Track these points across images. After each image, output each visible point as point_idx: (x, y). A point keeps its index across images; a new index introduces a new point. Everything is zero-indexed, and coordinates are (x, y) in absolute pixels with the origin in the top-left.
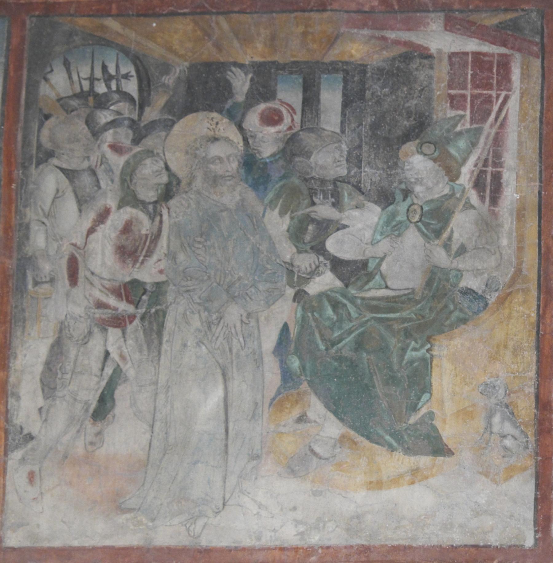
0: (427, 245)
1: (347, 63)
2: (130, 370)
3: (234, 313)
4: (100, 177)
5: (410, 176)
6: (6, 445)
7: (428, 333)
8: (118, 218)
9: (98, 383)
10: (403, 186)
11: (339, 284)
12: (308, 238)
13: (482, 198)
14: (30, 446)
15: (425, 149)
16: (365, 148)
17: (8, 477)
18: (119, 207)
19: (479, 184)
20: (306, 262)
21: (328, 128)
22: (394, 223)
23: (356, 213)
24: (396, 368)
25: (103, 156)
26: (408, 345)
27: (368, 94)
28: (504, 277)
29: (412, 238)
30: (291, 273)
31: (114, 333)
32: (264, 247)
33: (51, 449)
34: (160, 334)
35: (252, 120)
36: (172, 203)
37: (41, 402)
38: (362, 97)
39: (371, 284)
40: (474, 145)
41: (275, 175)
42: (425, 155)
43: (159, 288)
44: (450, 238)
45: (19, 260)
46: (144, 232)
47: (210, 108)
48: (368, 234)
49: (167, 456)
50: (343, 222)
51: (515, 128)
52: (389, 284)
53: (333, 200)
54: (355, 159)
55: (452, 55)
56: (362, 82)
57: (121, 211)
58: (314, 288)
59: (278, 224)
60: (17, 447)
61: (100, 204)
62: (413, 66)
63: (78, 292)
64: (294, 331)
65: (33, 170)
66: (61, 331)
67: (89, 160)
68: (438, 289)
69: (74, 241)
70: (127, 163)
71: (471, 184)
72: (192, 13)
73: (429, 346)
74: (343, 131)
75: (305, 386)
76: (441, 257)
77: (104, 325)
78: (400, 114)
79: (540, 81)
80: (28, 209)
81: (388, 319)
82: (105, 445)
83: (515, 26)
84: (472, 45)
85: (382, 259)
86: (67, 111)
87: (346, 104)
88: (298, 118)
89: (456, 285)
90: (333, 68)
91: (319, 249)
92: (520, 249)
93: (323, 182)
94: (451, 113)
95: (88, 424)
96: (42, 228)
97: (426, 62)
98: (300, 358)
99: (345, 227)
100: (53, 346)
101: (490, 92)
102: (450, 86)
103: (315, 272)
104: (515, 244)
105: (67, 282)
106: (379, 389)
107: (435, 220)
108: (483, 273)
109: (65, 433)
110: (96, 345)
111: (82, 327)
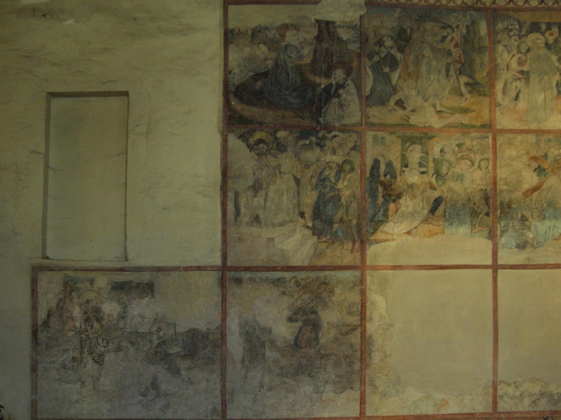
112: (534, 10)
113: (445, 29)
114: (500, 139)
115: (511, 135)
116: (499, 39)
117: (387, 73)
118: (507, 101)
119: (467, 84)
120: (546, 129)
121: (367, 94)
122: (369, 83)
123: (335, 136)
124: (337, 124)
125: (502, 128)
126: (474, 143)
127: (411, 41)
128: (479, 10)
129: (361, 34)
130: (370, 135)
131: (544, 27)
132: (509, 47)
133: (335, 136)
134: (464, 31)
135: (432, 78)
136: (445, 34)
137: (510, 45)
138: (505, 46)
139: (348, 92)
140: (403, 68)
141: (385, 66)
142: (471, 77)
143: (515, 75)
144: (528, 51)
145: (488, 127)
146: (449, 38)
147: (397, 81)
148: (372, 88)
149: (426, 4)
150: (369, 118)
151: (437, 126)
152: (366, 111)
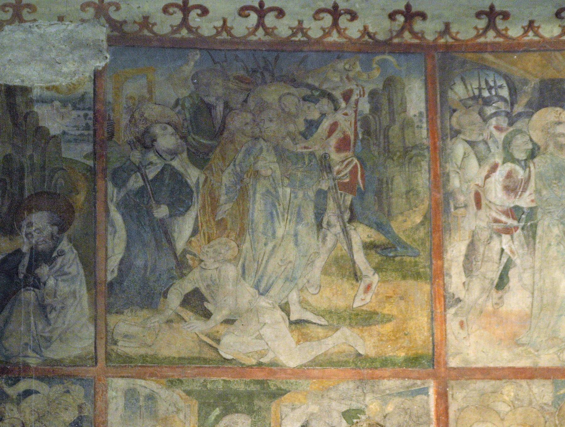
2: (517, 261)
6: (445, 305)
9: (498, 267)
14: (459, 305)
17: (447, 324)
18: (504, 163)
31: (506, 238)
33: (472, 307)
34: (534, 238)
37: (464, 279)
43: (532, 212)
45: (445, 194)
46: (520, 177)
49: (543, 312)
57: (505, 165)
60: (451, 306)
63: (482, 213)
66: (473, 236)
67: (482, 135)
69: (477, 183)
77: (499, 233)
80: (447, 165)
82: (505, 305)
86: (466, 107)
95: (494, 292)
96: (457, 175)
100: (469, 246)
105: (475, 208)
109: (479, 298)
110: (496, 245)
111: (486, 234)
113: (315, 101)
117: (162, 220)
118: (476, 291)
121: (109, 278)
122: (115, 247)
123: (27, 393)
124: (33, 361)
126: (390, 408)
127: (225, 134)
129: (96, 120)
130: (117, 386)
133: (27, 393)
135: (280, 232)
136: (315, 115)
137: (486, 143)
139: (61, 273)
140: (204, 207)
141: (158, 203)
146: (326, 124)
147: (189, 242)
148: (121, 262)
149: (267, 38)
150: (116, 343)
151: (293, 363)
152: (106, 325)
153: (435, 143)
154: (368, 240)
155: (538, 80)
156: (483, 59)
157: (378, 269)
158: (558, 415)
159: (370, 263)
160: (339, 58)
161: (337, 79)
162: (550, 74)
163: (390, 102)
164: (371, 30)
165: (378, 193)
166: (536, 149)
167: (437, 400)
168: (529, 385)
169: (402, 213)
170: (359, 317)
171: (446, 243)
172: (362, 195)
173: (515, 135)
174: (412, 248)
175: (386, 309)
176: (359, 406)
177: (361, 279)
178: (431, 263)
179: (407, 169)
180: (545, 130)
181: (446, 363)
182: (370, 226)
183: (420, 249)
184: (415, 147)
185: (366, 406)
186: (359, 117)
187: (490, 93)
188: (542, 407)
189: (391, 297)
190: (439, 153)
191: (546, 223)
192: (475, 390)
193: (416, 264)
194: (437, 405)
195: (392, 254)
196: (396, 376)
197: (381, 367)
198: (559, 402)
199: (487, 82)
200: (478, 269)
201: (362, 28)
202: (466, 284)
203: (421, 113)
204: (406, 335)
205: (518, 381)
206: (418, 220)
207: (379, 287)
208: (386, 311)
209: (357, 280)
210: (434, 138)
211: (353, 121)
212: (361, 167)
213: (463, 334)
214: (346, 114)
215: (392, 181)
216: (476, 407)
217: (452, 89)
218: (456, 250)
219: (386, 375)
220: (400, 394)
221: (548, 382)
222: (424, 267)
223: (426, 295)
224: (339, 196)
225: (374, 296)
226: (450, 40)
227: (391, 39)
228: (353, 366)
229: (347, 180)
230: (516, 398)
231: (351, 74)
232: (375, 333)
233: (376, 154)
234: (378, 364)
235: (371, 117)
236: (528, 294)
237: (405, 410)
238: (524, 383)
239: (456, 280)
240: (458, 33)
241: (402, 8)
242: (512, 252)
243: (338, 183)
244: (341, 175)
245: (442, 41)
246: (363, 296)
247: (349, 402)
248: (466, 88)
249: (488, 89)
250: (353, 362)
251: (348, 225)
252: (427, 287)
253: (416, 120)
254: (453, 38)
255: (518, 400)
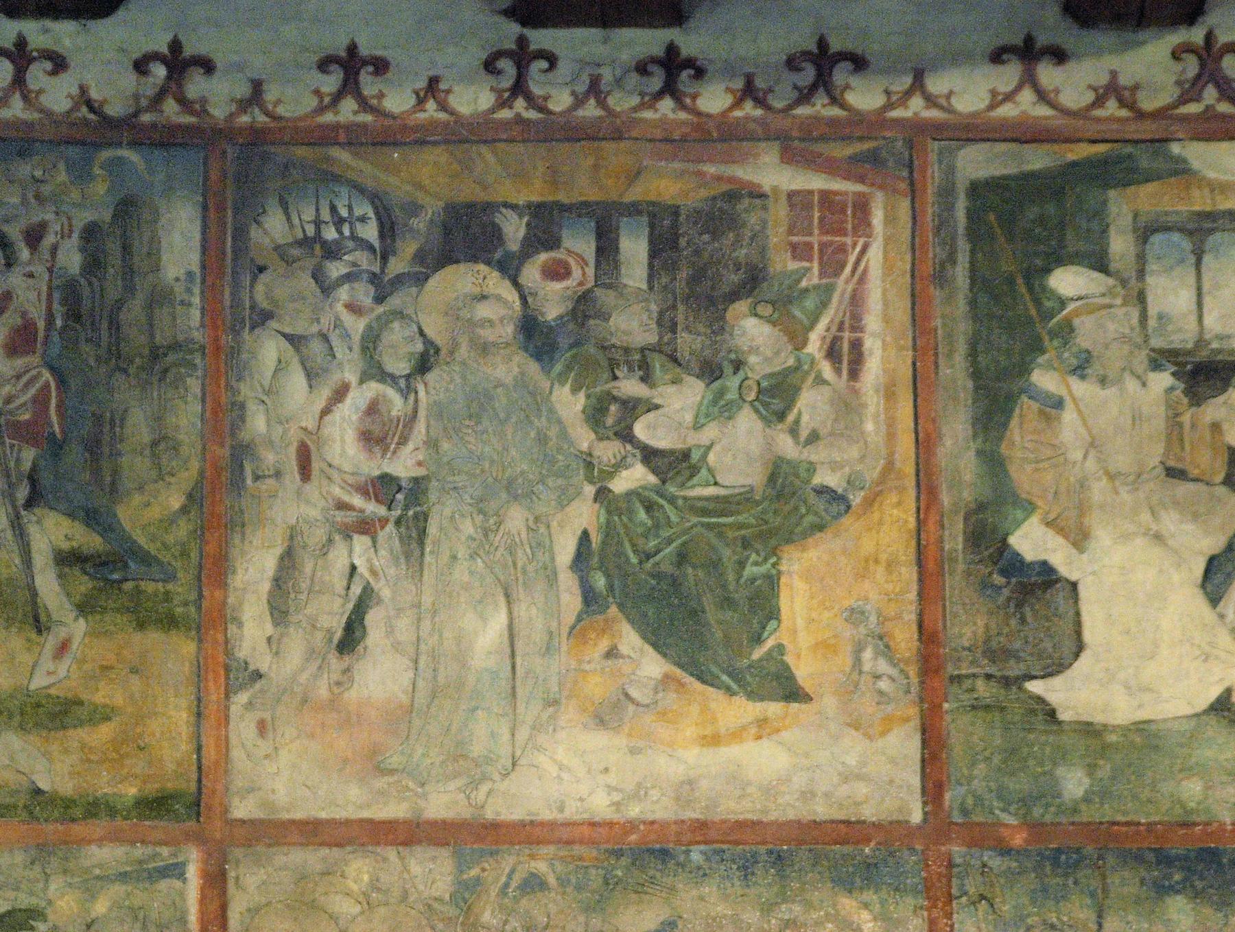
0: (767, 430)
1: (653, 204)
3: (516, 519)
4: (333, 344)
5: (742, 343)
7: (773, 542)
8: (359, 397)
9: (343, 605)
10: (733, 356)
11: (652, 479)
12: (610, 421)
13: (838, 371)
15: (760, 309)
16: (681, 308)
18: (362, 382)
19: (832, 353)
20: (608, 451)
21: (631, 283)
22: (723, 403)
23: (672, 389)
24: (731, 588)
25: (337, 318)
26: (748, 558)
27: (683, 242)
28: (872, 473)
29: (747, 422)
30: (589, 465)
31: (361, 543)
32: (553, 432)
33: (285, 690)
34: (421, 543)
35: (531, 274)
36: (431, 377)
37: (269, 629)
38: (675, 246)
39: (695, 480)
40: (824, 304)
41: (564, 342)
42: (761, 317)
44: (797, 422)
45: (233, 447)
46: (394, 413)
47: (474, 259)
48: (689, 418)
49: (436, 701)
50: (656, 401)
51: (878, 282)
52: (719, 479)
53: (641, 373)
54: (667, 324)
55: (791, 195)
56: (675, 226)
57: (364, 386)
58: (621, 484)
59: (569, 403)
61: (335, 378)
62: (740, 207)
63: (311, 489)
64: (596, 539)
65: (246, 334)
66: (292, 538)
67: (318, 322)
68: (783, 486)
69: (304, 424)
70: (369, 328)
71: (823, 353)
72: (447, 142)
73: (774, 559)
74: (651, 288)
75: (613, 610)
76: (787, 447)
77: (347, 533)
78: (726, 266)
79: (910, 225)
80: (242, 386)
81: (719, 525)
82: (355, 685)
83: (874, 158)
84: (817, 182)
85: (709, 448)
86: (287, 262)
87: (653, 254)
88: (590, 271)
89: (808, 481)
90: (634, 209)
91: (626, 436)
92: (891, 436)
93: (627, 350)
94: (793, 265)
95: (333, 658)
96: (261, 407)
97: (758, 201)
98: (608, 576)
99: (657, 407)
100: (282, 558)
101: (844, 239)
102: (790, 232)
103: (621, 464)
104: (883, 428)
105: (298, 477)
106: (712, 615)
107: (776, 399)
108: (843, 467)
109: (303, 669)
110: (339, 558)
111: (318, 535)
112: (462, 135)
114: (251, 883)
115: (312, 858)
116: (265, 305)
119: (67, 560)
120: (517, 815)
125: (260, 814)
126: (100, 907)
128: (165, 140)
131: (514, 229)
132: (316, 347)
134: (72, 259)
138: (295, 340)
142: (92, 518)
143: (342, 506)
144: (423, 365)
145: (180, 803)
153: (217, 339)
154: (65, 546)
155: (441, 204)
156: (328, 159)
157: (84, 608)
158: (462, 924)
159: (68, 595)
160: (22, 154)
161: (15, 200)
162: (468, 192)
163: (126, 249)
164: (94, 94)
165: (93, 447)
166: (432, 352)
167: (202, 889)
168: (402, 859)
169: (141, 488)
170: (41, 710)
171: (234, 552)
172: (56, 447)
173: (388, 322)
174: (159, 563)
175: (101, 693)
176: (34, 901)
177: (48, 629)
178: (201, 596)
179: (155, 394)
180: (452, 312)
181: (226, 811)
182: (71, 515)
183: (178, 564)
184: (175, 346)
185: (50, 902)
186: (56, 282)
187: (340, 232)
188: (429, 906)
189: (112, 668)
190: (226, 361)
191: (447, 512)
192: (286, 868)
193: (168, 597)
194: (203, 901)
195: (116, 576)
196: (115, 837)
197: (84, 818)
198: (467, 895)
199: (333, 209)
200: (298, 611)
201: (75, 91)
202: (274, 640)
203: (190, 274)
204: (141, 749)
205: (379, 850)
206: (176, 502)
207: (85, 645)
208: (99, 698)
209: (40, 632)
210: (215, 327)
211: (45, 288)
212: (58, 388)
213: (264, 747)
214: (31, 275)
215: (123, 420)
216: (288, 906)
217: (258, 223)
218: (255, 568)
219: (96, 836)
220: (123, 877)
221: (444, 853)
222: (186, 604)
223: (187, 664)
224: (8, 452)
225: (74, 666)
226: (262, 118)
227: (136, 114)
228: (25, 815)
229: (27, 417)
230: (375, 885)
231: (46, 189)
232: (76, 744)
233: (92, 362)
234: (78, 812)
235: (83, 281)
236: (407, 662)
237: (134, 912)
238: (391, 853)
239: (252, 631)
240: (278, 102)
241: (165, 50)
242: (374, 572)
243: (7, 424)
244: (12, 406)
245: (245, 119)
246: (50, 666)
247: (11, 894)
248: (289, 219)
249: (335, 224)
250: (25, 807)
251: (23, 513)
252: (189, 648)
253: (179, 289)
254: (267, 114)
255: (379, 890)
